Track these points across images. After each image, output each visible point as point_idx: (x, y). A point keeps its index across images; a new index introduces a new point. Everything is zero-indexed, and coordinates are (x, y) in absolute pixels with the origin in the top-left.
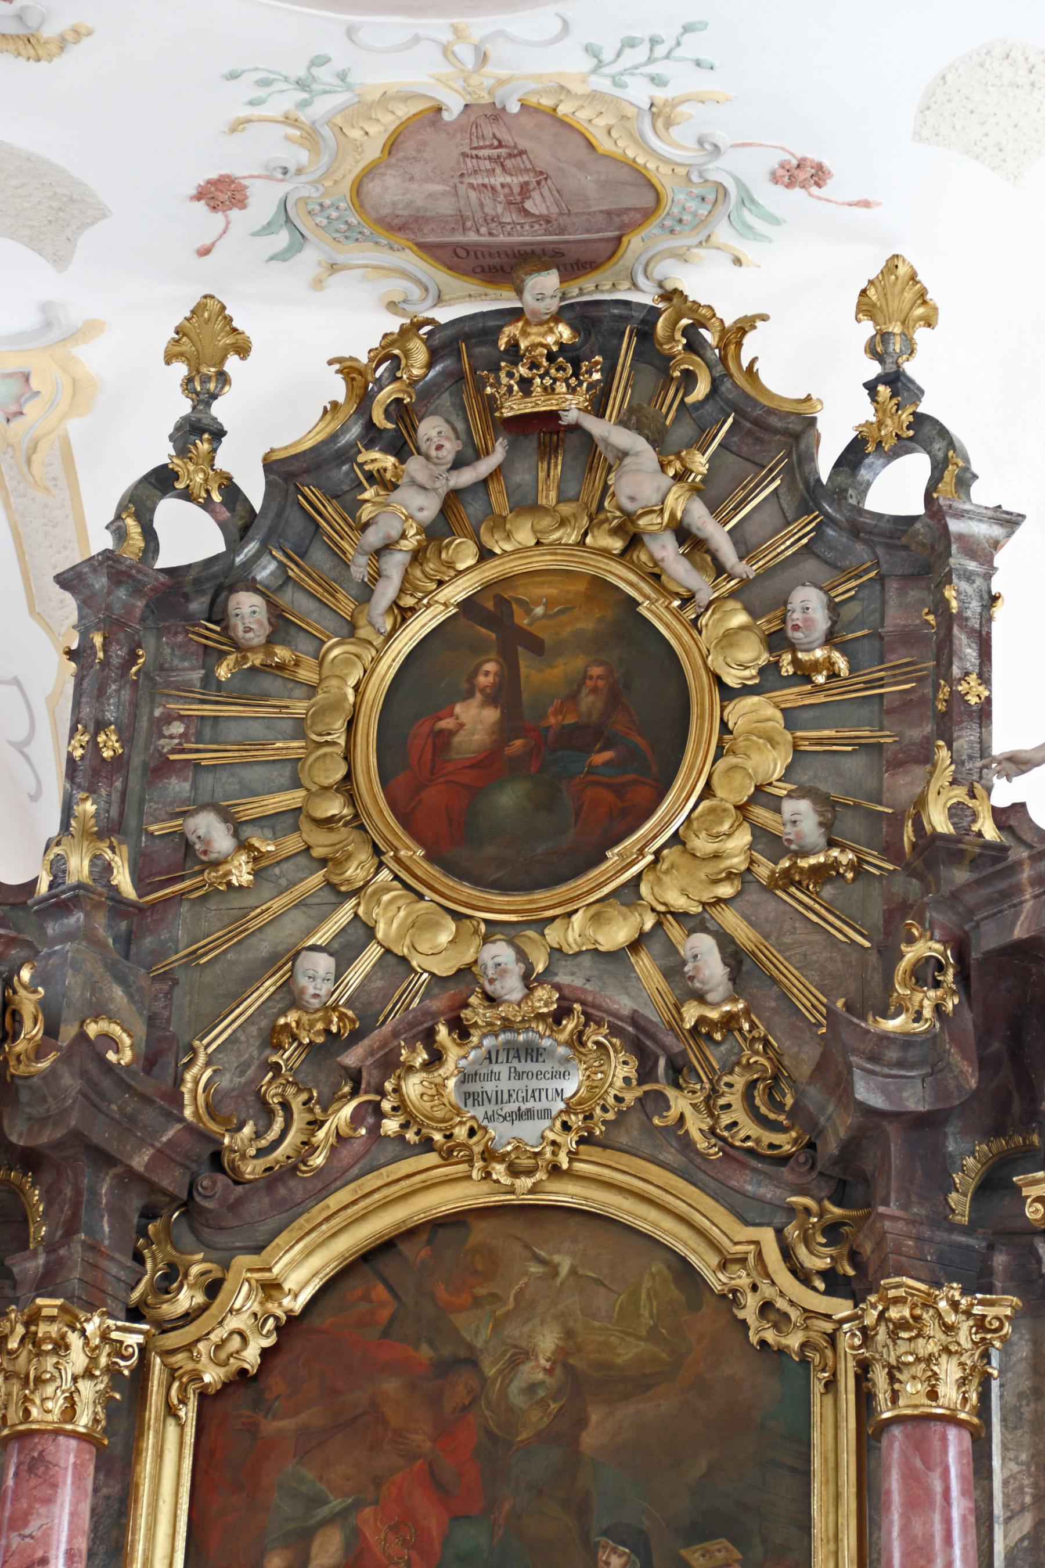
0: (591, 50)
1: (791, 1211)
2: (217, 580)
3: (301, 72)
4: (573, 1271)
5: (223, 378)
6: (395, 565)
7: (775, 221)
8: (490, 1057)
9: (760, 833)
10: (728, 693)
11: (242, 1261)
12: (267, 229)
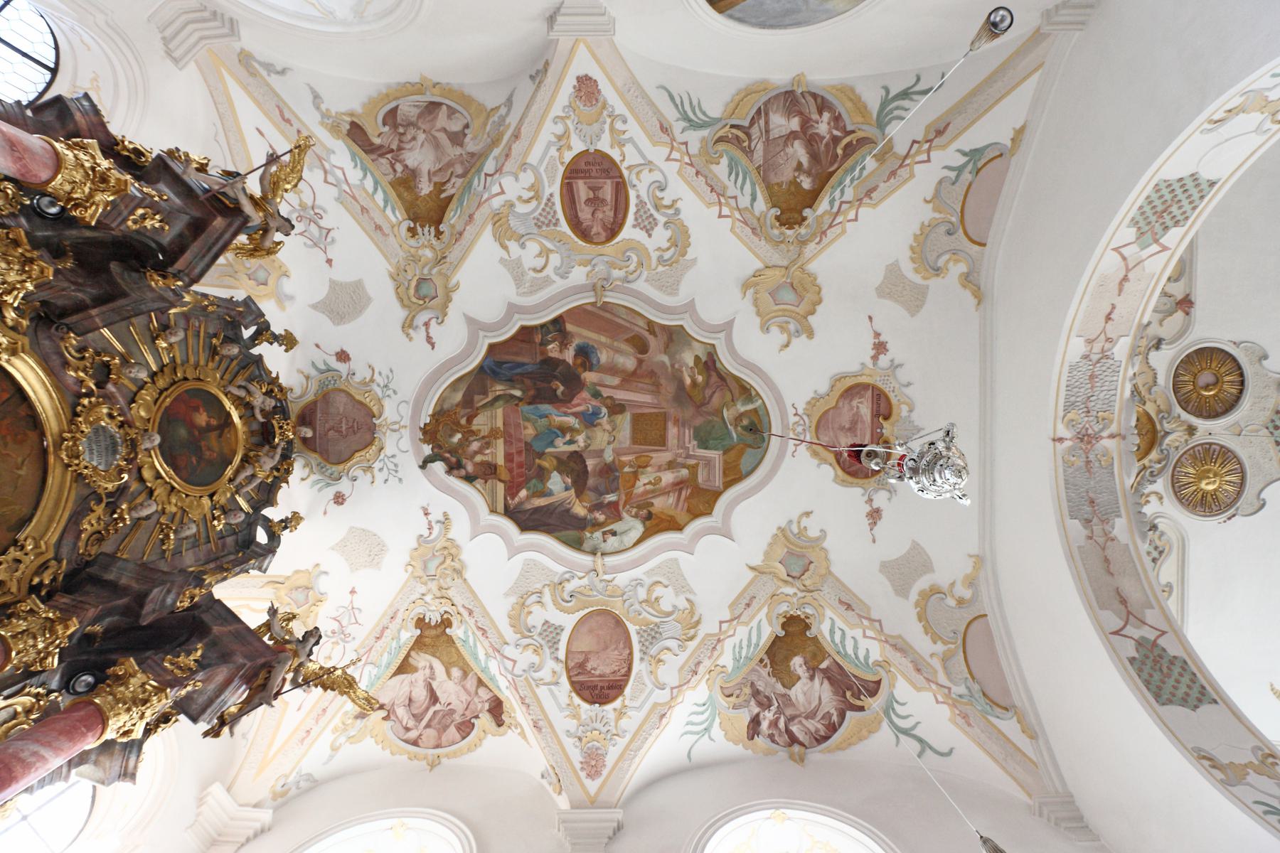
0: (393, 456)
1: (59, 561)
2: (235, 339)
3: (391, 386)
4: (20, 476)
6: (242, 393)
7: (320, 490)
8: (112, 437)
9: (175, 514)
10: (211, 496)
11: (26, 340)
12: (325, 363)
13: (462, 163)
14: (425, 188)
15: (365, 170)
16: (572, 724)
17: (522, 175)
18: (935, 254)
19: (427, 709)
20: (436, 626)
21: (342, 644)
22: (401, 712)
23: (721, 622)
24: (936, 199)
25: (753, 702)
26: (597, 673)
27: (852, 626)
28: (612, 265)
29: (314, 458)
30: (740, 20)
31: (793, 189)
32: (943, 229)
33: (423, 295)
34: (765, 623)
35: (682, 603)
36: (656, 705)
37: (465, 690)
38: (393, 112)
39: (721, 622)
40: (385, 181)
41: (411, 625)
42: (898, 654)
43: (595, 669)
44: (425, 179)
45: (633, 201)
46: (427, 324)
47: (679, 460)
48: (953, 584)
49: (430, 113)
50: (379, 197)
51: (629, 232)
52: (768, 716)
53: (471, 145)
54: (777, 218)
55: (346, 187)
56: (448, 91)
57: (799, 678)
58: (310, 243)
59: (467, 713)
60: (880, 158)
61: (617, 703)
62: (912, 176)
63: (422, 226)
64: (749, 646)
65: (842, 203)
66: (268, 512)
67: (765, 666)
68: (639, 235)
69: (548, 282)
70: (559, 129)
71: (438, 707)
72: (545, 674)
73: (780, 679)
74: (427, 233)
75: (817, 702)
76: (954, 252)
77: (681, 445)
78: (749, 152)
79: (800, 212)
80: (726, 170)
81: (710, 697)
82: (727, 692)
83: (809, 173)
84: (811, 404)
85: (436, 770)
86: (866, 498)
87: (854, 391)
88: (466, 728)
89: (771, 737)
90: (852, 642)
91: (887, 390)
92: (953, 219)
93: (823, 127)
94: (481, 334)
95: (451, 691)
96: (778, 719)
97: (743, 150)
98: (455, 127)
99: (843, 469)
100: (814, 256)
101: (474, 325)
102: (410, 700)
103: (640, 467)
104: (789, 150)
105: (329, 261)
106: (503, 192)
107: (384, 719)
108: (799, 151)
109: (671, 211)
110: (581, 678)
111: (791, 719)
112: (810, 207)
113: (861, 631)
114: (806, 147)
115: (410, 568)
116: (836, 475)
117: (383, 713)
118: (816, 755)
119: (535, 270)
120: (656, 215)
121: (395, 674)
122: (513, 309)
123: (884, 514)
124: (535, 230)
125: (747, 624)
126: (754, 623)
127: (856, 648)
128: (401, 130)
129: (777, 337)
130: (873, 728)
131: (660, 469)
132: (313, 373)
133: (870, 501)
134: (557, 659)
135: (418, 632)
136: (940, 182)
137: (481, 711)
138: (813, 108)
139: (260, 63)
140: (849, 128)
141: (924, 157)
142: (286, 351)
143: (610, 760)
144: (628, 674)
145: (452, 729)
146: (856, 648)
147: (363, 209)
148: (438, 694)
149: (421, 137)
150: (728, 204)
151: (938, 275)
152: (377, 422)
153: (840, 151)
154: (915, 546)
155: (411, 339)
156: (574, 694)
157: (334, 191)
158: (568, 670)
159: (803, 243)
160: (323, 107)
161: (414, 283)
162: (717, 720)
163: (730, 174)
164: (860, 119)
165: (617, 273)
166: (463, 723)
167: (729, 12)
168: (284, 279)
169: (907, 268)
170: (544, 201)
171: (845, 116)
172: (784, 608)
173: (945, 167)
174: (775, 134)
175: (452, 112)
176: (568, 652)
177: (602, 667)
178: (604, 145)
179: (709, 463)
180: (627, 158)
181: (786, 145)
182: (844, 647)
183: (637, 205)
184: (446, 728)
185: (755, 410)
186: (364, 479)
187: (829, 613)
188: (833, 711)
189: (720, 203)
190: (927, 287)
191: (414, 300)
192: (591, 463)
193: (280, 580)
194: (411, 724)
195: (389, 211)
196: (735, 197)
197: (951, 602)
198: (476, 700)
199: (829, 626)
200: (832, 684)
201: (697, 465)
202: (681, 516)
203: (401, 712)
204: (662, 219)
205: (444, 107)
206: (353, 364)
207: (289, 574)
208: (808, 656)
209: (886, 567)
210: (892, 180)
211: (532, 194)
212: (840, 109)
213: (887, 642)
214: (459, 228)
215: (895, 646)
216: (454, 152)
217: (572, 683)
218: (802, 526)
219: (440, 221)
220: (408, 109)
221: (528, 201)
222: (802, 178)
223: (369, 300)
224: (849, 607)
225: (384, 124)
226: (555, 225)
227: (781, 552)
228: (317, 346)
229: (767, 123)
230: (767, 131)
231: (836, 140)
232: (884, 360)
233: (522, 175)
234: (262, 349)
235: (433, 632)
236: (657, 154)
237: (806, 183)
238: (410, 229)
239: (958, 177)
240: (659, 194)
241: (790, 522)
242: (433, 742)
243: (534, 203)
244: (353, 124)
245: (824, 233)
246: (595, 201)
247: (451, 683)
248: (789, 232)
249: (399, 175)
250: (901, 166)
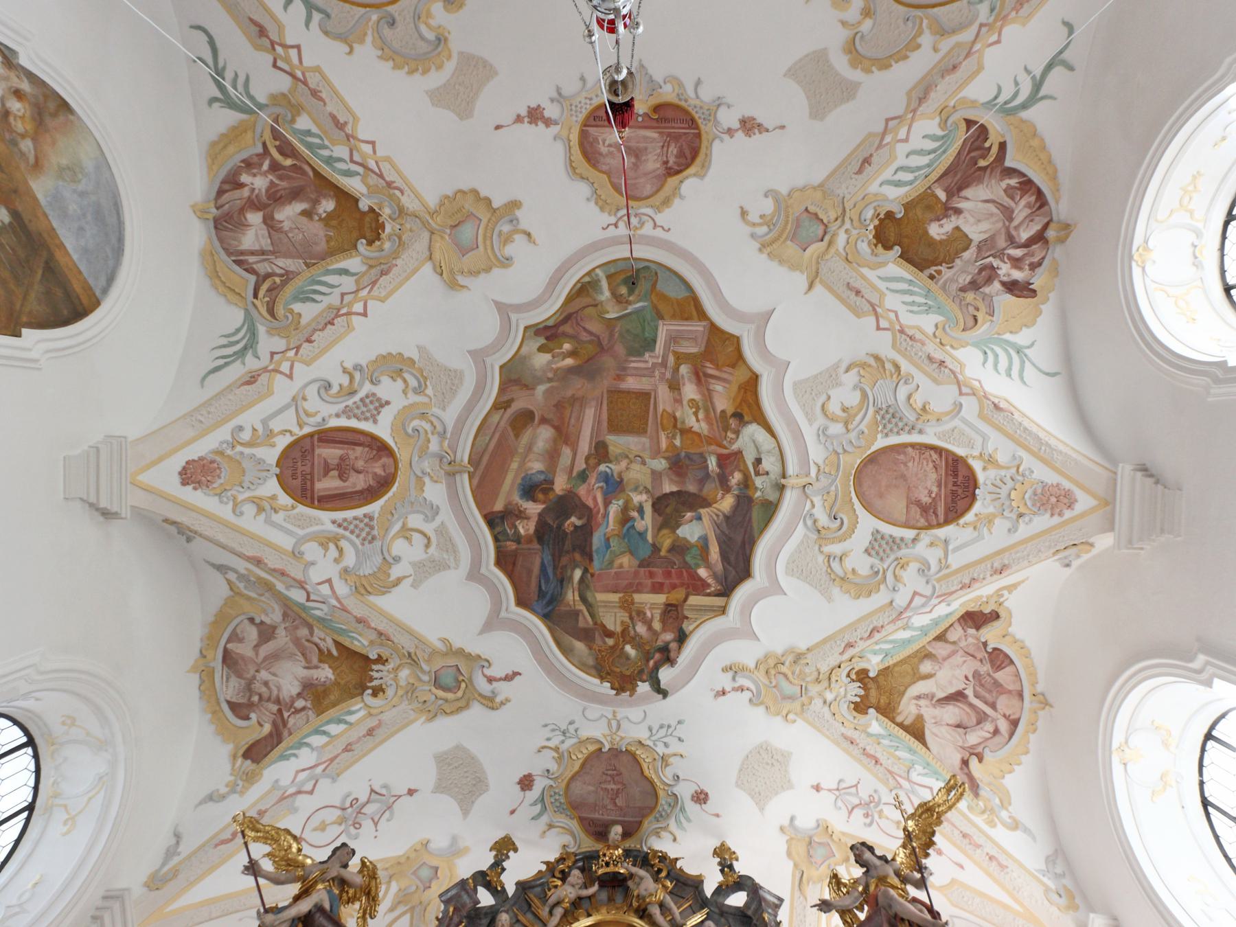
0: (650, 729)
3: (563, 727)
5: (508, 857)
6: (559, 912)
7: (689, 820)
12: (534, 804)
13: (296, 628)
14: (325, 673)
15: (301, 745)
16: (1001, 525)
17: (308, 557)
18: (421, 43)
19: (971, 705)
20: (865, 688)
21: (881, 807)
22: (973, 738)
23: (878, 328)
24: (349, 39)
25: (987, 290)
26: (935, 489)
27: (892, 157)
28: (423, 451)
29: (648, 824)
30: (111, 279)
31: (334, 223)
32: (387, 31)
33: (455, 682)
34: (882, 272)
35: (851, 378)
36: (981, 416)
37: (949, 656)
38: (233, 706)
39: (878, 328)
40: (315, 721)
41: (862, 719)
42: (932, 95)
43: (930, 492)
44: (315, 674)
45: (343, 422)
46: (490, 680)
47: (668, 375)
48: (844, 23)
49: (236, 663)
50: (334, 729)
51: (382, 429)
52: (1006, 270)
53: (274, 616)
54: (370, 243)
55: (319, 769)
56: (210, 640)
57: (957, 228)
58: (387, 814)
59: (979, 656)
60: (297, 110)
61: (977, 466)
62: (317, 69)
63: (372, 679)
64: (911, 293)
65: (352, 161)
66: (709, 889)
67: (939, 272)
68: (386, 416)
69: (442, 531)
70: (250, 509)
71: (969, 693)
72: (933, 555)
73: (957, 254)
74: (380, 674)
75: (992, 208)
76: (417, 17)
77: (649, 372)
78: (288, 276)
79: (364, 214)
80: (309, 305)
81: (976, 345)
82: (971, 322)
83: (316, 202)
84: (603, 205)
85: (1051, 700)
86: (726, 137)
87: (589, 151)
88: (998, 659)
89: (1033, 267)
90: (912, 157)
91: (590, 108)
92: (375, 17)
93: (259, 183)
94: (503, 614)
95: (950, 675)
96: (1010, 258)
97: (284, 283)
98: (252, 634)
99: (688, 166)
100: (418, 196)
101: (493, 623)
102: (958, 726)
103: (675, 426)
104: (286, 225)
105: (411, 792)
106: (329, 581)
107: (980, 760)
108: (288, 213)
109: (357, 376)
110: (941, 510)
111: (1011, 240)
112: (357, 201)
113: (899, 145)
114: (283, 204)
115: (791, 716)
116: (695, 175)
117: (974, 762)
118: (1061, 208)
119: (427, 546)
121: (924, 744)
122: (475, 575)
123: (748, 114)
124: (378, 543)
125: (882, 295)
126: (882, 285)
127: (921, 153)
128: (255, 699)
129: (518, 247)
130: (1030, 133)
131: (678, 401)
132: (545, 819)
133: (730, 132)
134: (914, 540)
135: (872, 711)
136: (326, 33)
137: (978, 639)
138: (236, 194)
139: (163, 865)
140: (260, 150)
142: (516, 850)
143: (1051, 478)
144: (939, 450)
145: (1001, 676)
146: (921, 153)
147: (348, 749)
148: (952, 690)
149: (264, 675)
150: (350, 304)
151: (446, 40)
152: (607, 747)
154: (792, 73)
155: (508, 700)
156: (962, 521)
157: (324, 784)
158: (930, 527)
159: (401, 212)
160: (223, 790)
161: (440, 693)
162: (1007, 336)
163: (314, 300)
164: (249, 135)
165: (434, 446)
166: (992, 662)
167: (98, 293)
168: (432, 846)
169: (436, 79)
170: (341, 531)
171: (244, 155)
172: (864, 247)
173: (307, 25)
174: (266, 243)
175: (235, 637)
176: (907, 525)
177: (928, 482)
178: (270, 456)
179: (673, 339)
180: (288, 428)
181: (280, 230)
182: (919, 168)
183: (349, 418)
184: (996, 684)
185: (609, 277)
186: (677, 767)
187: (874, 188)
188: (1004, 184)
189: (349, 314)
190: (461, 53)
191: (460, 694)
192: (668, 487)
193: (798, 875)
194: (989, 727)
195: (352, 719)
196: (343, 295)
197: (867, 25)
198: (963, 644)
199: (889, 189)
200: (967, 186)
201: (675, 353)
202: (740, 376)
203: (973, 738)
204: (367, 388)
205: (229, 646)
206: (536, 771)
207: (791, 864)
208: (929, 215)
209: (818, 112)
210: (324, 95)
211: (332, 546)
212: (237, 159)
213: (914, 111)
214: (374, 636)
215: (921, 101)
216: (282, 638)
217: (947, 522)
218: (758, 220)
219: (366, 658)
220: (230, 689)
221: (341, 551)
222: (321, 211)
223: (459, 748)
224: (867, 161)
225: (247, 718)
226: (371, 518)
227: (791, 249)
228: (512, 812)
229: (253, 253)
230: (263, 253)
231: (275, 167)
232: (551, 111)
233: (308, 557)
234: (509, 882)
235: (873, 693)
236: (283, 390)
237: (328, 205)
238: (375, 694)
239: (319, 10)
240: (335, 389)
241: (753, 236)
242: (1015, 701)
243: (344, 544)
244: (246, 755)
245: (389, 184)
246: (343, 468)
247: (940, 675)
248: (388, 229)
249: (309, 705)
250: (305, 83)
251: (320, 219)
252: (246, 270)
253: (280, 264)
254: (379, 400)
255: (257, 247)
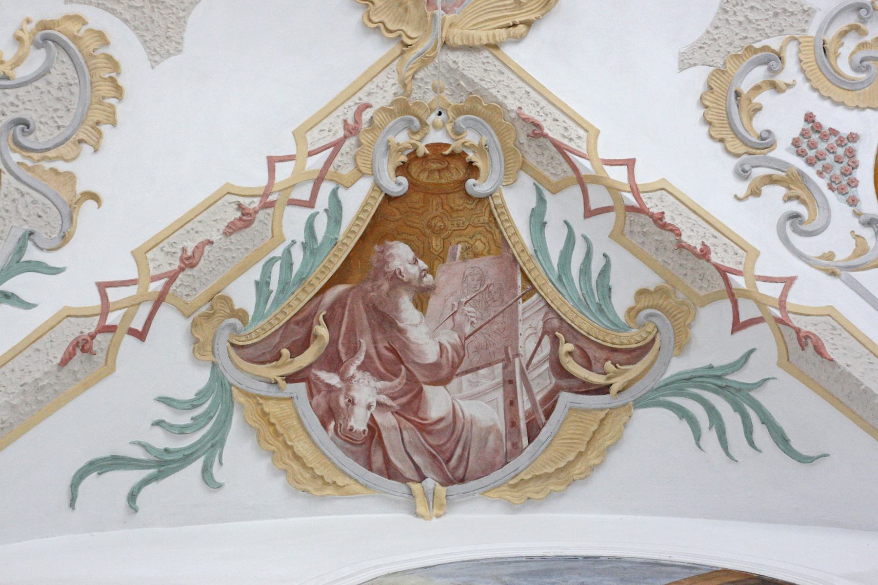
18: (55, 77)
24: (72, 205)
31: (436, 244)
32: (41, 137)
54: (472, 169)
60: (218, 305)
62: (140, 255)
65: (310, 204)
78: (556, 329)
79: (412, 184)
80: (615, 279)
83: (396, 279)
93: (365, 392)
97: (573, 333)
100: (370, 76)
104: (449, 338)
112: (388, 198)
114: (406, 346)
120: (799, 163)
136: (65, 238)
138: (390, 439)
140: (300, 388)
141: (114, 294)
150: (613, 189)
151: (44, 25)
153: (322, 330)
159: (403, 108)
163: (605, 271)
164: (270, 407)
169: (125, 45)
171: (312, 421)
173: (56, 271)
181: (460, 352)
183: (853, 183)
189: (635, 190)
196: (589, 213)
204: (783, 152)
210: (190, 247)
212: (324, 437)
222: (414, 271)
229: (512, 403)
231: (332, 360)
237: (401, 256)
239: (21, 249)
240: (795, 207)
245: (351, 130)
248: (436, 137)
250: (172, 277)
251: (431, 271)
252: (548, 414)
253: (531, 346)
254: (804, 134)
255: (499, 394)
